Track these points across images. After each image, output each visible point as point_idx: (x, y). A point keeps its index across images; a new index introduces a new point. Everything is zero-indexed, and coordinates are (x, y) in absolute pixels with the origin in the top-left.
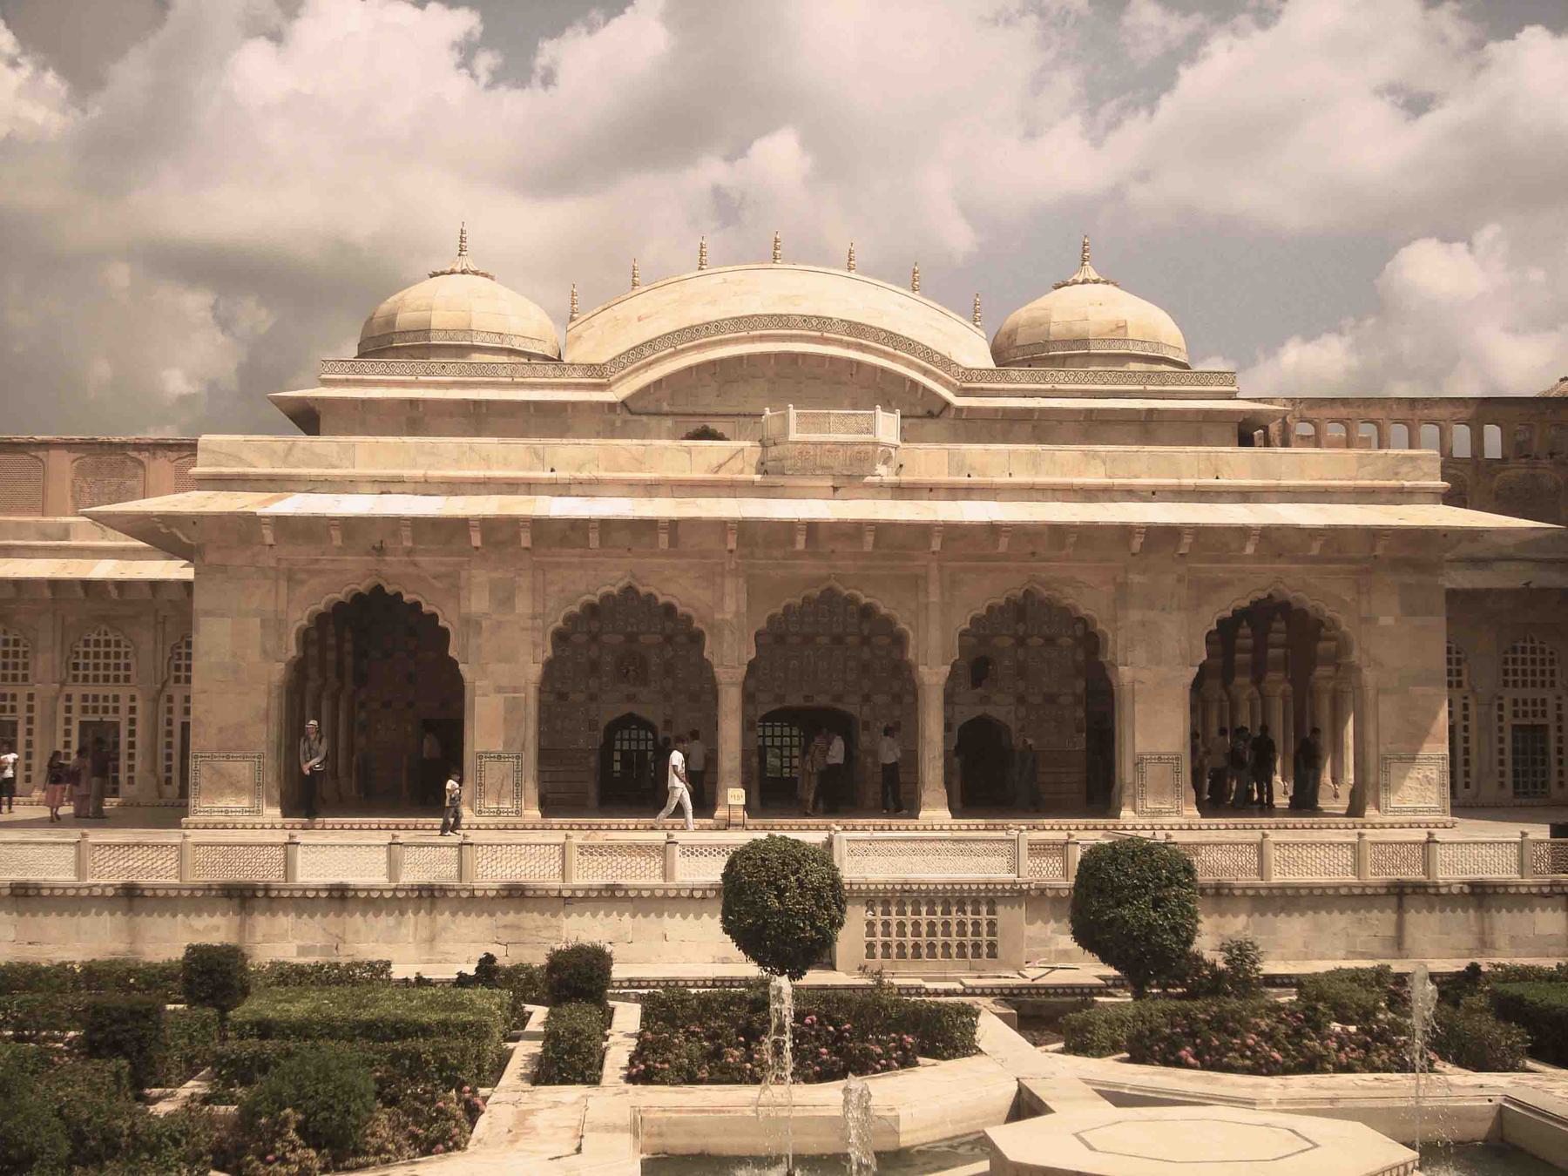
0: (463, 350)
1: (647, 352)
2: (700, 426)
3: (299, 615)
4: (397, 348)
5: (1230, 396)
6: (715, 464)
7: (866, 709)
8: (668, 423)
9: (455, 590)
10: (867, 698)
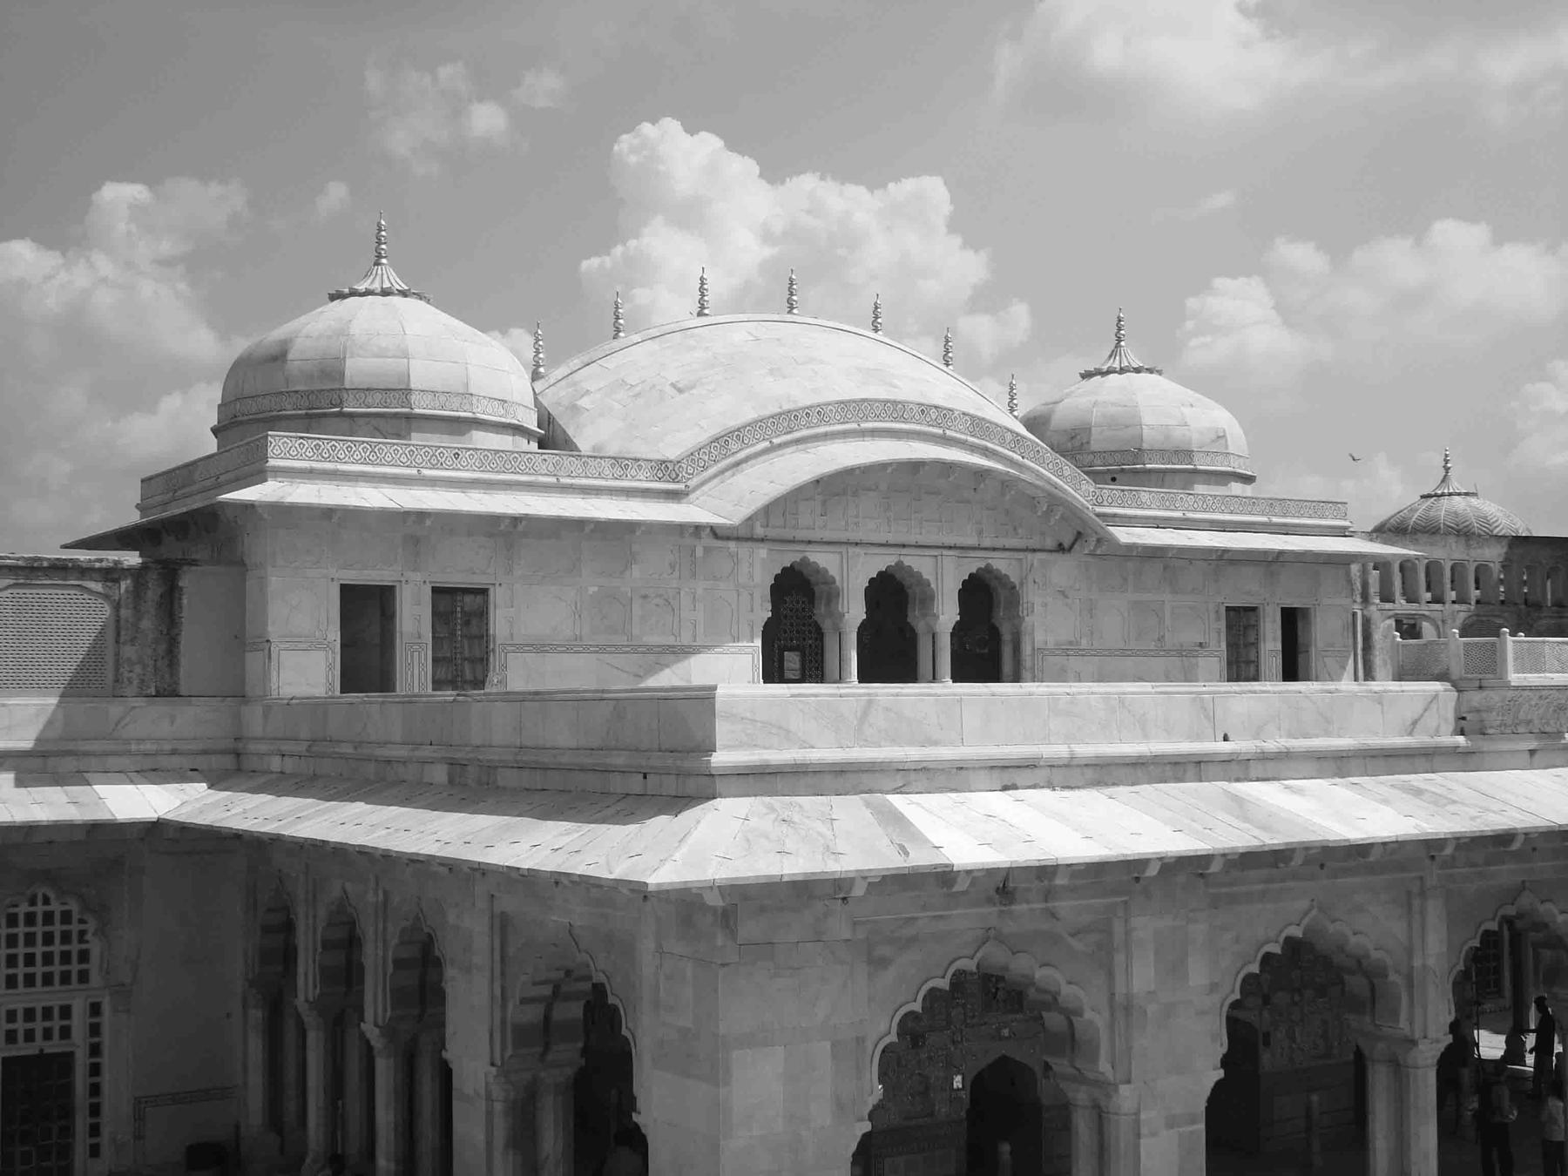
0: (460, 425)
1: (734, 447)
2: (797, 558)
3: (883, 1027)
4: (351, 416)
5: (1342, 532)
6: (1410, 716)
7: (1266, 1014)
8: (762, 552)
9: (1105, 954)
10: (1266, 1000)
